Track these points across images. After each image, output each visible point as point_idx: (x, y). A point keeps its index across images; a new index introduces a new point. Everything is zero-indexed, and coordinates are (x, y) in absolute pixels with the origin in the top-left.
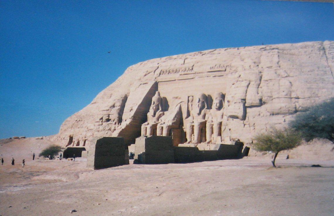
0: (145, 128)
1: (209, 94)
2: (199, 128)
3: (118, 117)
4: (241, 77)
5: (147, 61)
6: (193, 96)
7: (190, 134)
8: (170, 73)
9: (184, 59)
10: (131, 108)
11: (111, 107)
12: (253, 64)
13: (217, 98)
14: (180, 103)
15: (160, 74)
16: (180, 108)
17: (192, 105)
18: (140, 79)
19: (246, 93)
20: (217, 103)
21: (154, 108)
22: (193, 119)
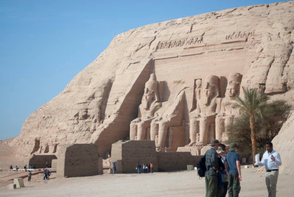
0: (135, 127)
1: (222, 76)
2: (206, 125)
3: (99, 113)
4: (263, 51)
5: (141, 27)
6: (201, 79)
7: (194, 132)
8: (171, 47)
9: (190, 24)
10: (117, 99)
11: (90, 98)
12: (284, 31)
13: (232, 82)
14: (183, 89)
15: (157, 48)
16: (184, 96)
17: (200, 91)
18: (130, 56)
19: (267, 74)
20: (231, 89)
21: (148, 97)
22: (200, 112)
